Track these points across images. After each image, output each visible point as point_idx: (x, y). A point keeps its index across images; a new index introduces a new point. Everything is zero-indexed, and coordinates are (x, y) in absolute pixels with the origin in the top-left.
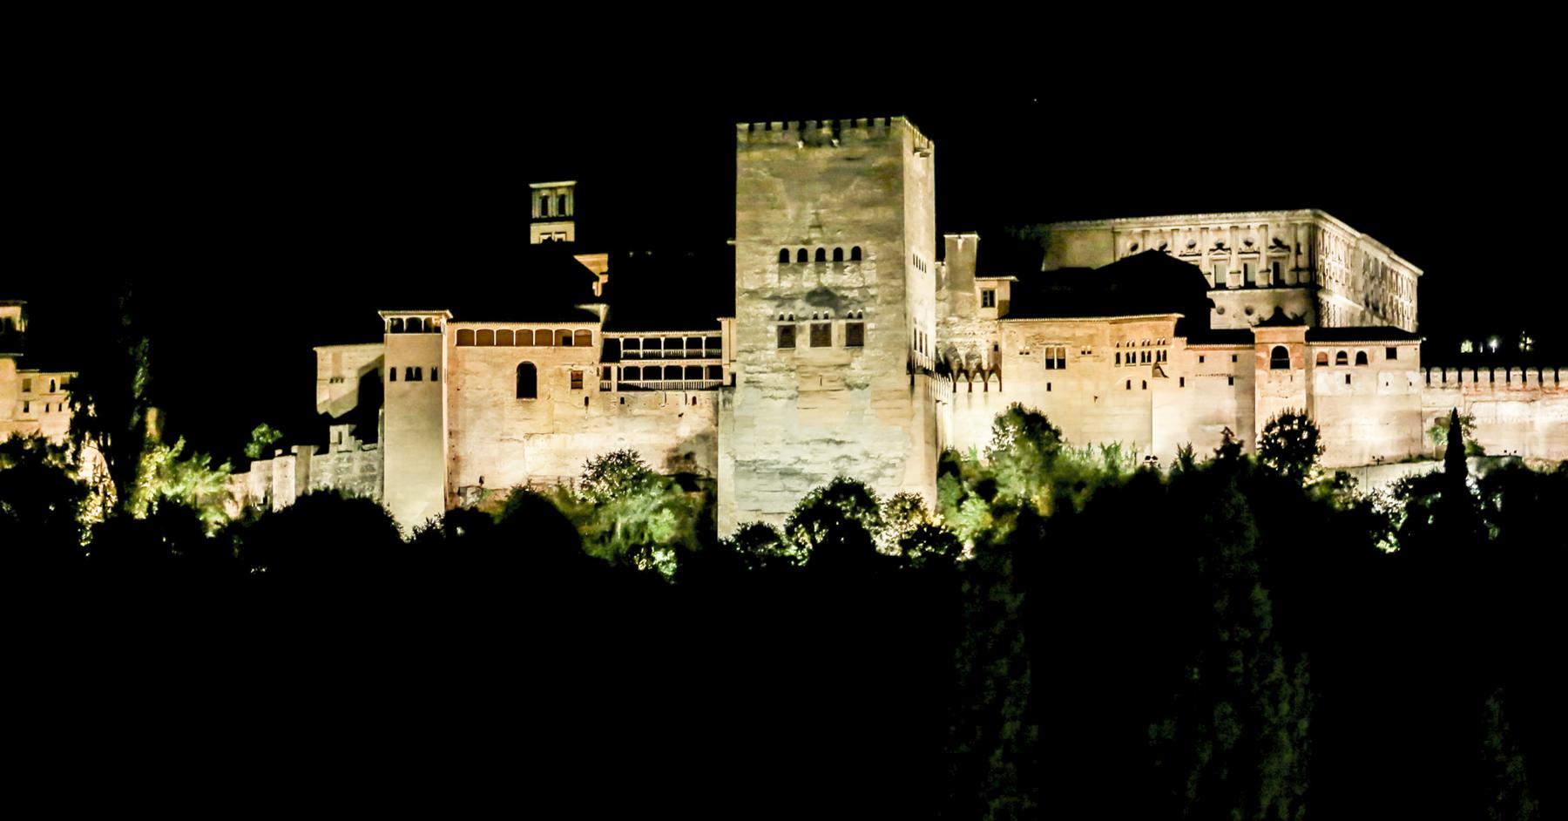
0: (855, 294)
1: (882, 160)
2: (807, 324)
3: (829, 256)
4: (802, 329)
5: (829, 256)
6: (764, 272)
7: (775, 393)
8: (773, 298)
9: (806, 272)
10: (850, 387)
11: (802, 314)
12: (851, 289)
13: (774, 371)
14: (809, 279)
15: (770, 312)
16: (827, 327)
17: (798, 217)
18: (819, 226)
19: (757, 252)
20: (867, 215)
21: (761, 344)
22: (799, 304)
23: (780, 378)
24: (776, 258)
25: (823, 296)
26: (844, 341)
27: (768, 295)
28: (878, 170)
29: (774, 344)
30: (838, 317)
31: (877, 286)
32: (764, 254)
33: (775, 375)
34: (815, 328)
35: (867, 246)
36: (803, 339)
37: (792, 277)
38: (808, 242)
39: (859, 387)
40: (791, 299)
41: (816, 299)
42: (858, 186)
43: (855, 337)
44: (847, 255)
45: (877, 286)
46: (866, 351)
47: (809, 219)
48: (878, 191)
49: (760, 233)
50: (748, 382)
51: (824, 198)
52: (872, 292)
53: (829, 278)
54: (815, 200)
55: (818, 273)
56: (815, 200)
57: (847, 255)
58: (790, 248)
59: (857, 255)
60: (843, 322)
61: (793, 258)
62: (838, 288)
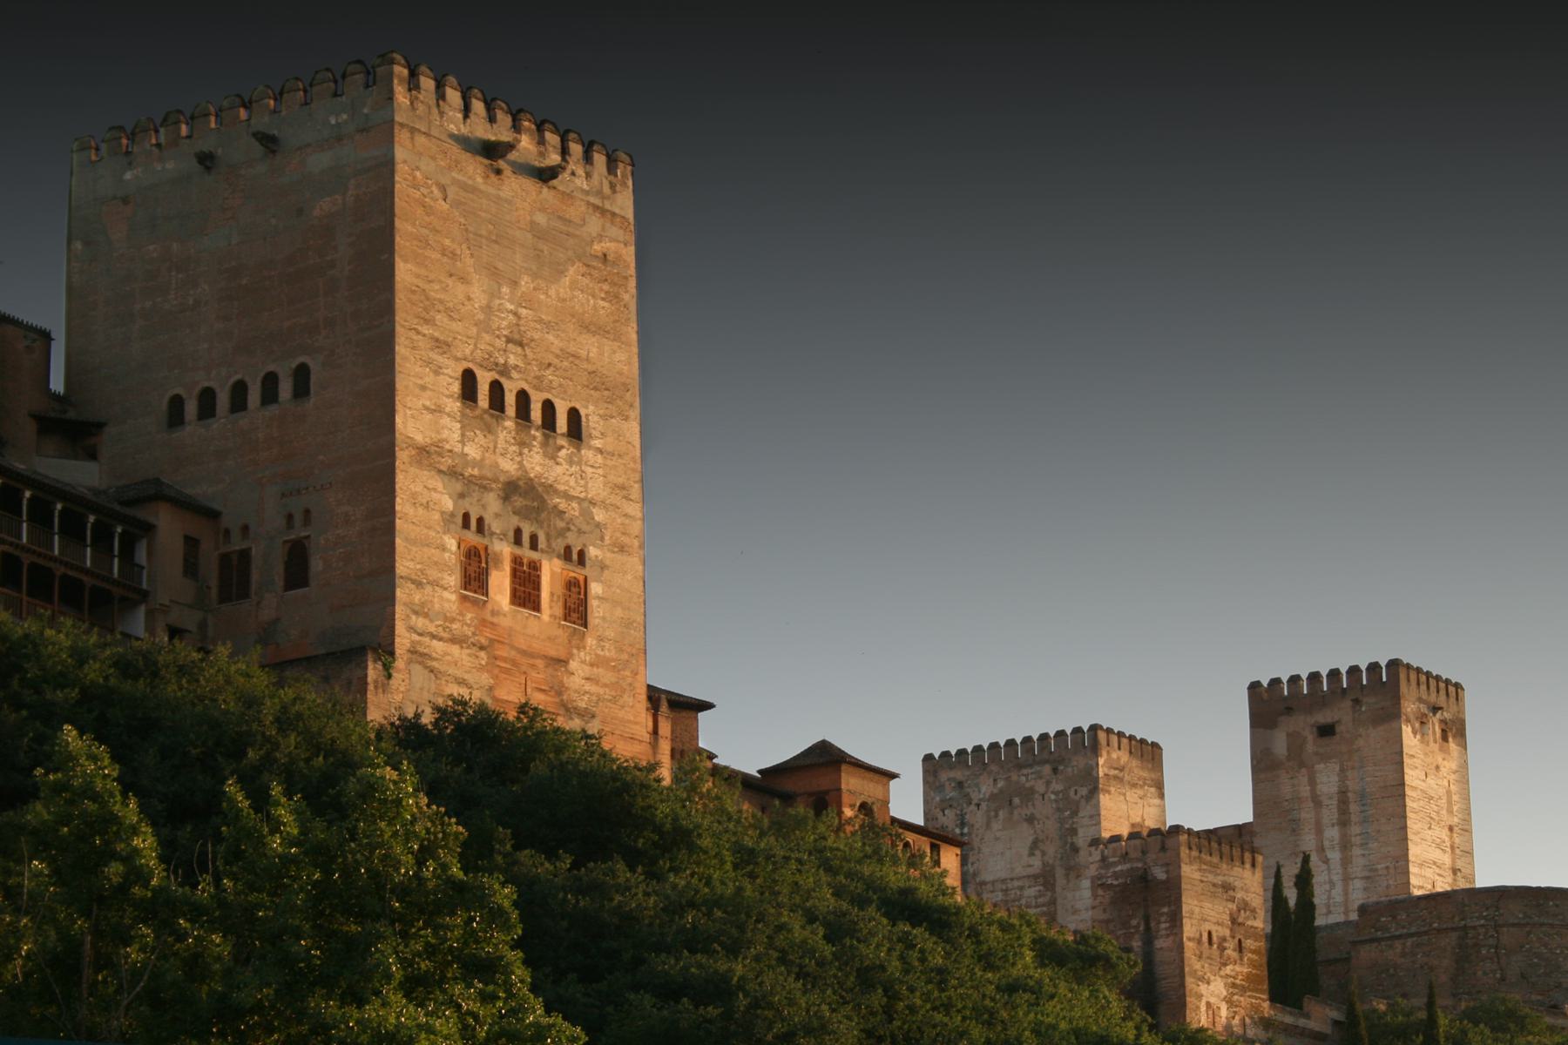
0: (573, 509)
3: (536, 413)
5: (536, 413)
8: (453, 473)
9: (502, 436)
12: (568, 497)
13: (453, 640)
17: (488, 309)
18: (521, 344)
19: (428, 363)
21: (433, 574)
24: (456, 387)
26: (559, 611)
27: (446, 463)
29: (453, 580)
30: (549, 551)
31: (605, 505)
33: (455, 650)
37: (480, 439)
38: (505, 370)
41: (519, 502)
42: (574, 285)
44: (562, 423)
46: (590, 641)
47: (504, 322)
50: (413, 652)
51: (525, 283)
52: (599, 515)
53: (535, 462)
54: (514, 284)
55: (522, 444)
57: (562, 423)
58: (479, 373)
62: (550, 489)
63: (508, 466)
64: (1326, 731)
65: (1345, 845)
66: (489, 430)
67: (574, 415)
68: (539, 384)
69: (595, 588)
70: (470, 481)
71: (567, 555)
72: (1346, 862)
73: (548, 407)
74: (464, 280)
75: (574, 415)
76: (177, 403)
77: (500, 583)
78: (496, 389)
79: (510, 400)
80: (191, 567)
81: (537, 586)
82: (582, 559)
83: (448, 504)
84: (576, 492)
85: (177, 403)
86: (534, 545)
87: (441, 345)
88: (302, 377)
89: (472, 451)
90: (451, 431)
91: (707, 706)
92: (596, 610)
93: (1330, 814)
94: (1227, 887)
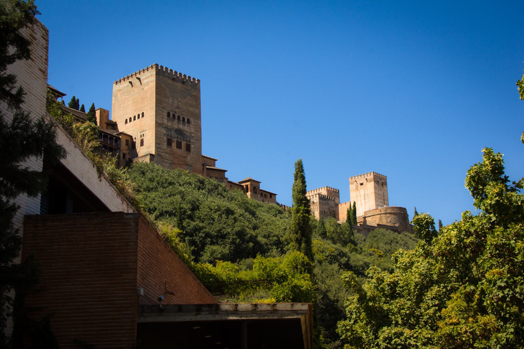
0: (188, 134)
1: (194, 93)
2: (175, 140)
3: (181, 119)
4: (174, 141)
5: (181, 119)
6: (163, 118)
7: (167, 161)
8: (166, 128)
10: (187, 165)
11: (174, 136)
12: (187, 132)
14: (175, 125)
15: (165, 132)
16: (181, 143)
17: (172, 103)
20: (191, 109)
21: (162, 143)
22: (173, 132)
23: (168, 156)
24: (166, 114)
25: (179, 132)
26: (185, 149)
27: (164, 126)
28: (194, 96)
29: (165, 144)
30: (184, 140)
31: (194, 133)
32: (163, 112)
34: (177, 142)
35: (192, 120)
36: (174, 145)
38: (176, 112)
39: (189, 165)
40: (171, 130)
42: (189, 99)
43: (188, 148)
44: (186, 121)
45: (194, 133)
47: (176, 105)
48: (194, 103)
49: (162, 104)
52: (193, 135)
53: (181, 126)
54: (177, 99)
56: (177, 99)
57: (186, 121)
59: (189, 122)
60: (185, 142)
61: (171, 117)
62: (184, 131)
63: (176, 127)
64: (362, 184)
65: (365, 203)
66: (172, 121)
67: (188, 120)
68: (182, 115)
69: (192, 146)
70: (168, 129)
71: (187, 141)
72: (365, 206)
73: (184, 118)
74: (168, 98)
75: (188, 120)
76: (126, 120)
77: (174, 145)
78: (174, 116)
79: (176, 117)
80: (127, 144)
81: (181, 146)
82: (189, 142)
83: (165, 132)
84: (189, 131)
85: (126, 120)
86: (181, 139)
87: (163, 108)
88: (143, 114)
89: (169, 124)
90: (165, 121)
91: (226, 171)
92: (192, 150)
93: (363, 198)
94: (328, 203)
